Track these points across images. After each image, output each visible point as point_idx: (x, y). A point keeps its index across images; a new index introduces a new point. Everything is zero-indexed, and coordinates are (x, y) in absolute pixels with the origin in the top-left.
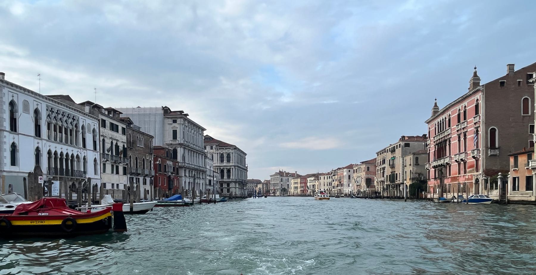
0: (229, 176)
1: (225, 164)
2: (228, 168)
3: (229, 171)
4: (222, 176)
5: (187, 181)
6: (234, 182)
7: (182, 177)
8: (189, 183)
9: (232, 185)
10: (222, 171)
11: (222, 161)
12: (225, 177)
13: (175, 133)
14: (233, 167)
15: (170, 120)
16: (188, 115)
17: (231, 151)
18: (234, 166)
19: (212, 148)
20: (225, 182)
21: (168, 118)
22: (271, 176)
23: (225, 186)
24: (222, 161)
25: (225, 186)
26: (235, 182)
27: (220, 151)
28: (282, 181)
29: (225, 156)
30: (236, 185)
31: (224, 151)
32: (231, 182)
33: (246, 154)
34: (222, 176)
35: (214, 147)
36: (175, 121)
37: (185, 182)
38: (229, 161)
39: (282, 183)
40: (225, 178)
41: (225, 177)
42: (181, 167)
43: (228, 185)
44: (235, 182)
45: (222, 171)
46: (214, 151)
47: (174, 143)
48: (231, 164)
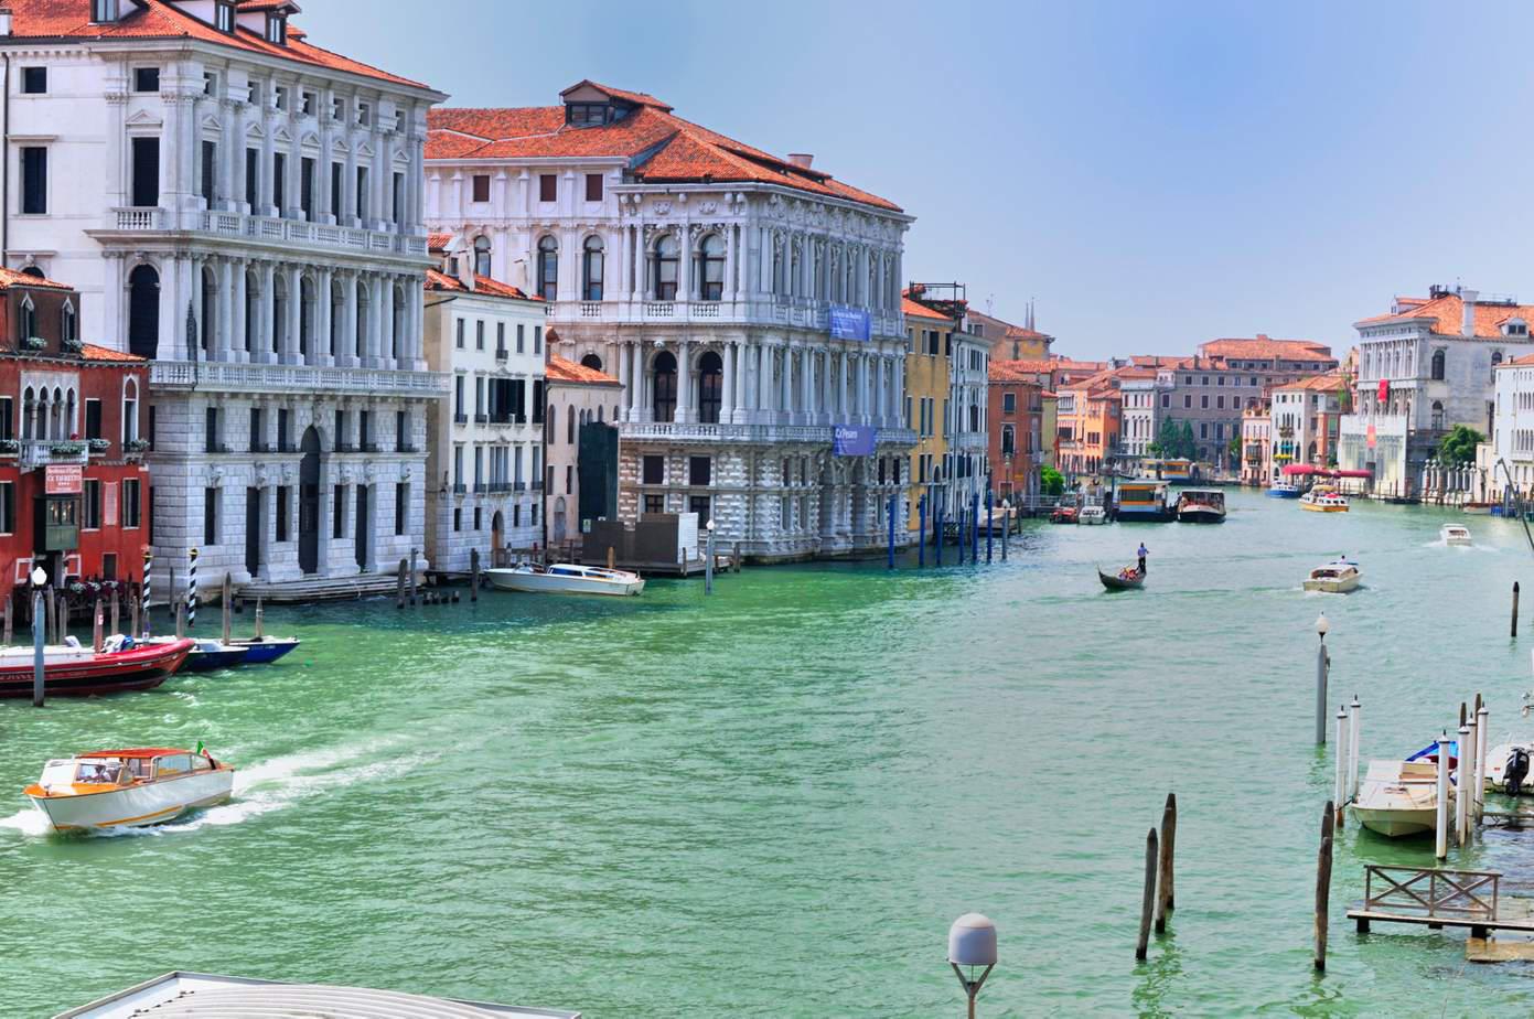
0: (708, 406)
1: (680, 313)
2: (704, 339)
3: (709, 364)
4: (663, 404)
5: (235, 483)
6: (740, 449)
7: (176, 458)
8: (255, 496)
9: (729, 474)
10: (663, 365)
11: (663, 291)
12: (684, 409)
13: (145, 154)
14: (741, 339)
15: (115, 70)
16: (291, 10)
17: (724, 215)
18: (751, 330)
19: (594, 190)
20: (677, 449)
21: (106, 57)
22: (1365, 330)
23: (677, 475)
24: (663, 291)
25: (677, 475)
26: (754, 453)
27: (647, 215)
28: (1438, 372)
29: (684, 246)
30: (754, 473)
31: (681, 216)
32: (722, 448)
33: (893, 218)
34: (663, 404)
35: (612, 180)
36: (147, 81)
37: (212, 495)
38: (709, 291)
39: (1437, 391)
40: (680, 412)
41: (684, 409)
42: (179, 396)
43: (700, 470)
44: (754, 453)
45: (663, 365)
46: (608, 207)
47: (134, 229)
48: (723, 314)
